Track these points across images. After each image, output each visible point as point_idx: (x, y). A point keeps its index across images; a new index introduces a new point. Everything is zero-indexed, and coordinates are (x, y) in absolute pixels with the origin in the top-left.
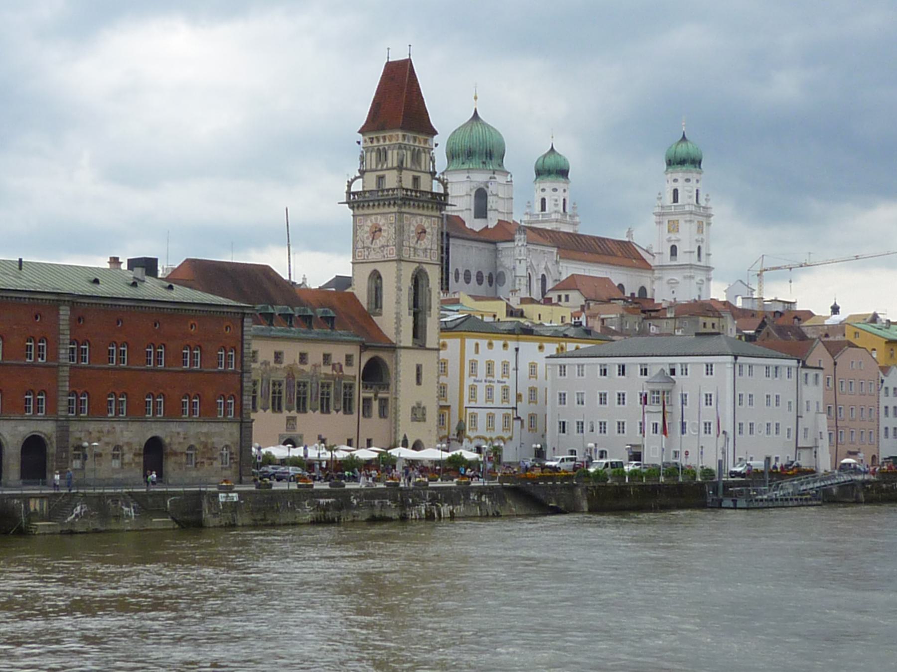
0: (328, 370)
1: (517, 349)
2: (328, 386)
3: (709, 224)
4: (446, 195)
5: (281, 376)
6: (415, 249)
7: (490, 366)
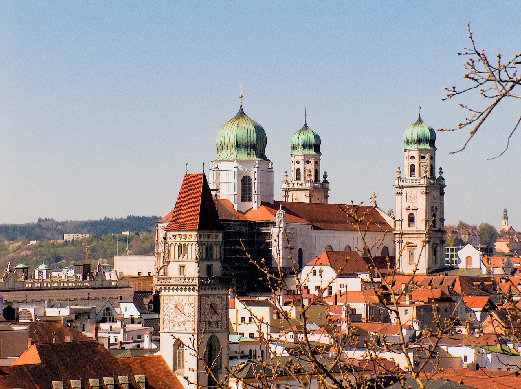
6: (209, 323)
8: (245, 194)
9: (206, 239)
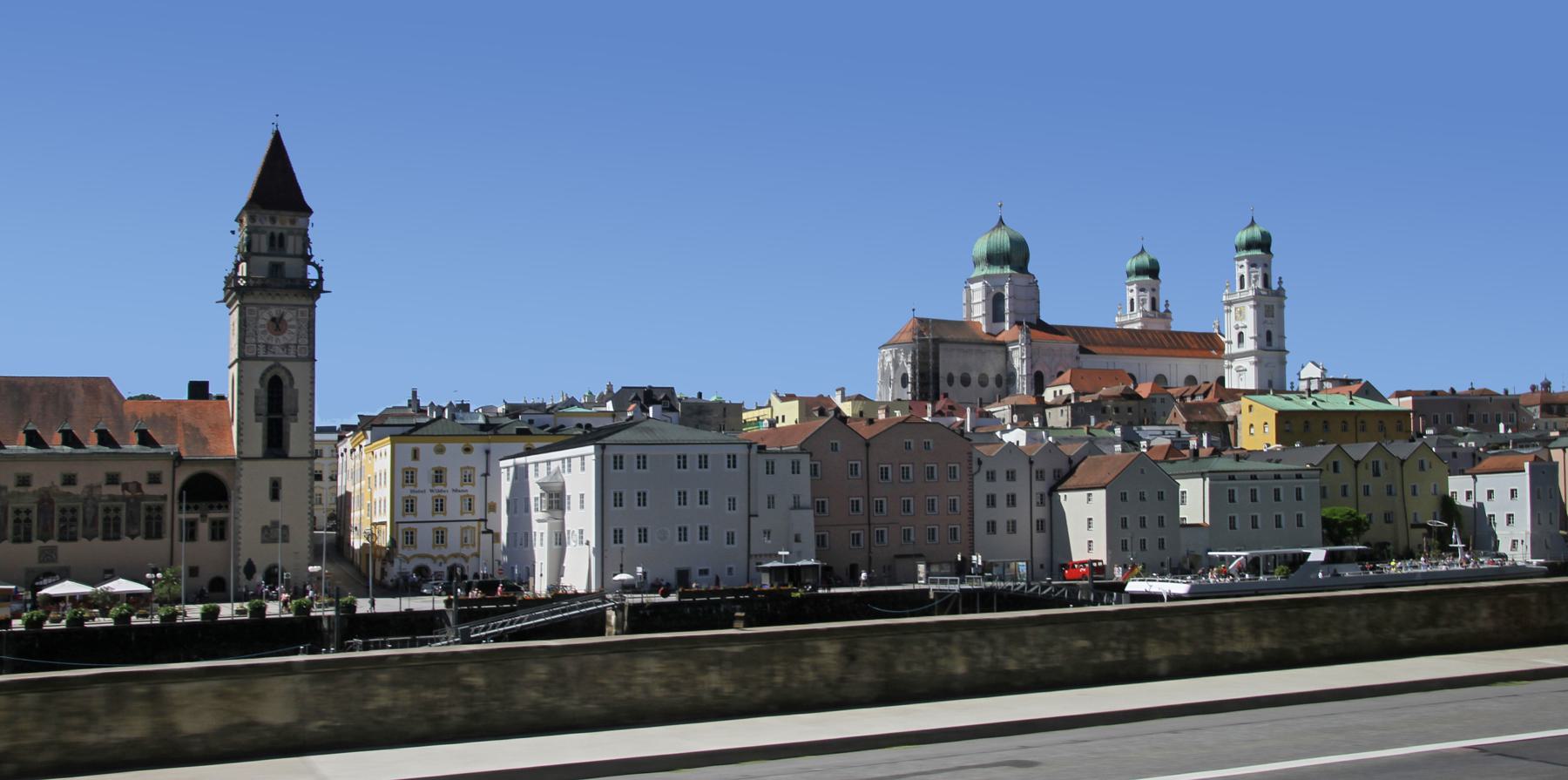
0: (116, 490)
1: (488, 452)
2: (117, 510)
3: (1282, 306)
4: (320, 280)
5: (30, 502)
6: (267, 347)
7: (439, 476)
8: (996, 314)
9: (268, 224)
